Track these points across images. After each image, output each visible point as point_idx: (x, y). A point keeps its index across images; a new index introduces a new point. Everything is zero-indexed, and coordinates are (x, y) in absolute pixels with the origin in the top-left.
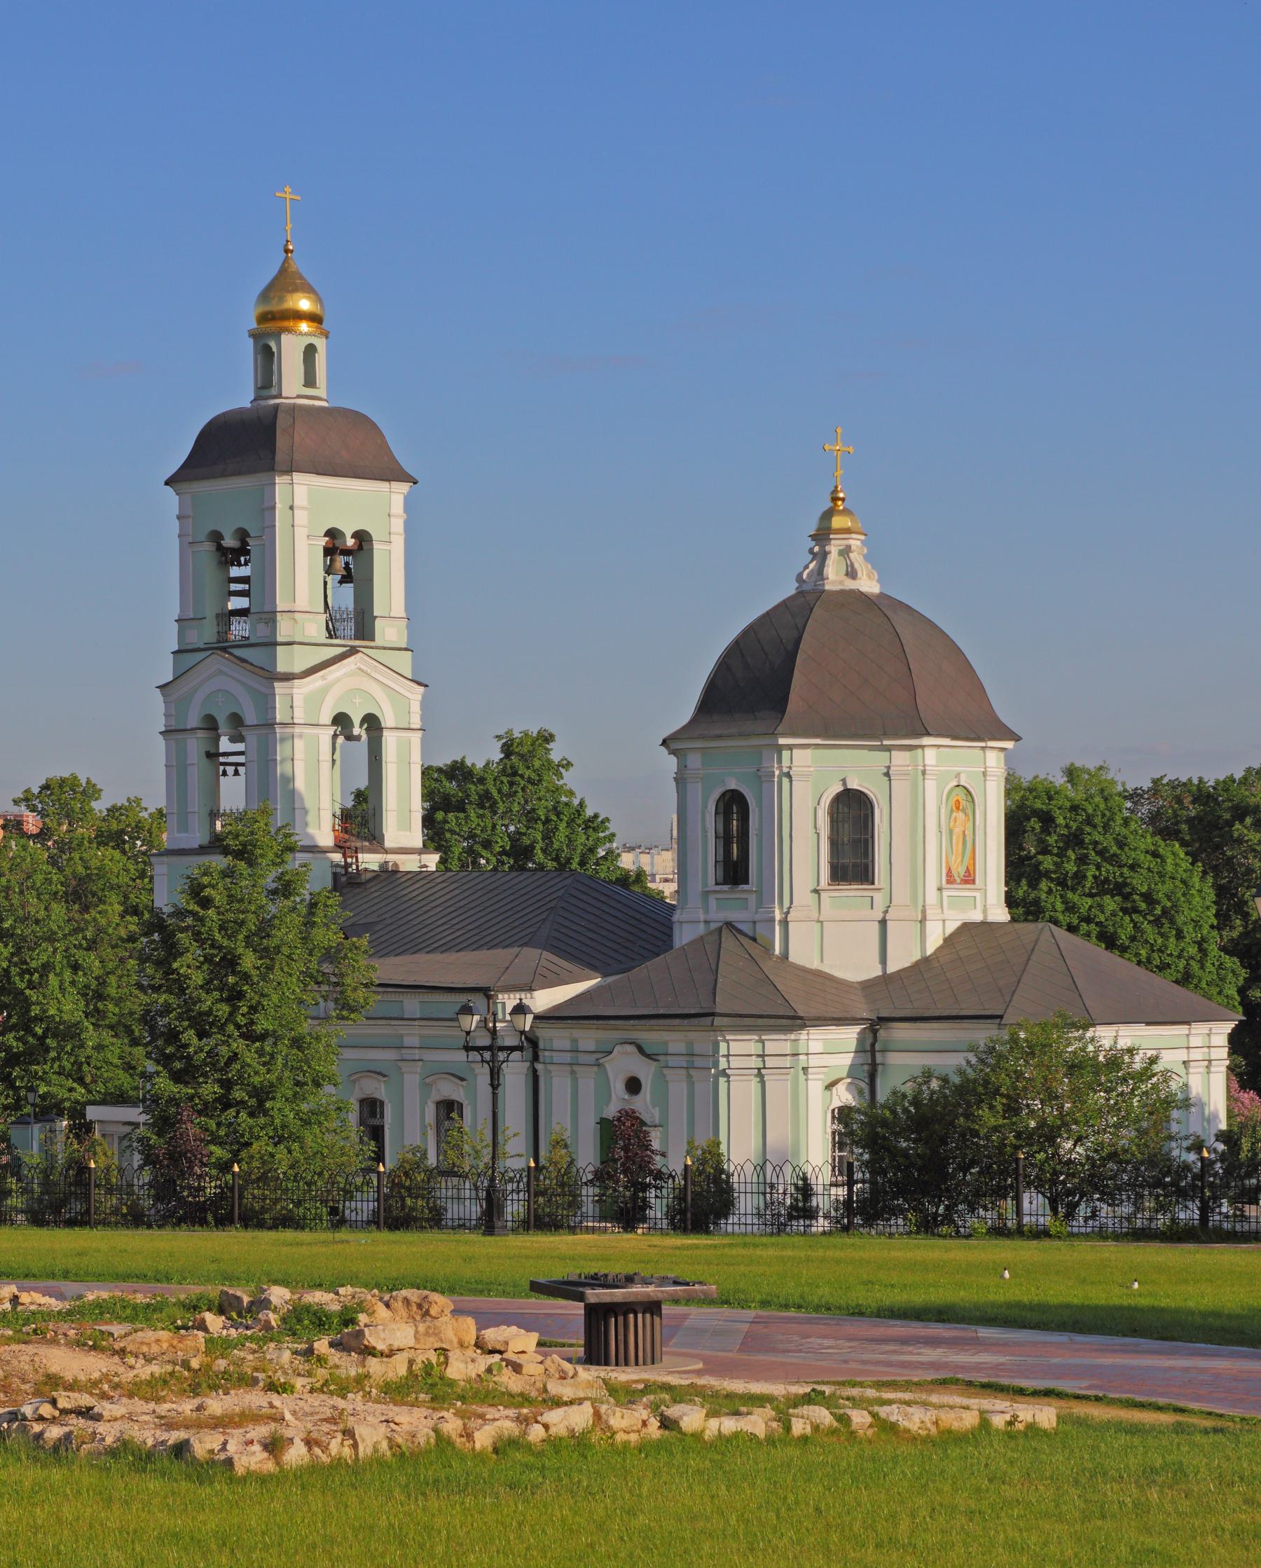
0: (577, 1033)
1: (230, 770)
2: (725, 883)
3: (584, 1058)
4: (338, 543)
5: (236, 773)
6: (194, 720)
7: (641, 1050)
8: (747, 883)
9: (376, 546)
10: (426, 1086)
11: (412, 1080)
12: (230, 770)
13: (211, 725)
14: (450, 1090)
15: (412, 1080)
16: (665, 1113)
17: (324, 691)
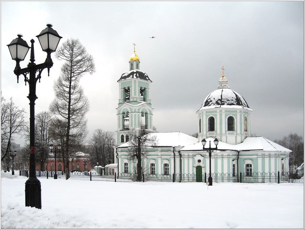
0: (189, 153)
1: (126, 120)
2: (210, 131)
3: (190, 157)
4: (142, 89)
5: (126, 121)
6: (121, 112)
7: (201, 156)
8: (214, 130)
9: (147, 90)
10: (162, 162)
11: (160, 160)
12: (126, 120)
13: (124, 113)
14: (166, 162)
15: (160, 160)
16: (205, 165)
17: (140, 108)
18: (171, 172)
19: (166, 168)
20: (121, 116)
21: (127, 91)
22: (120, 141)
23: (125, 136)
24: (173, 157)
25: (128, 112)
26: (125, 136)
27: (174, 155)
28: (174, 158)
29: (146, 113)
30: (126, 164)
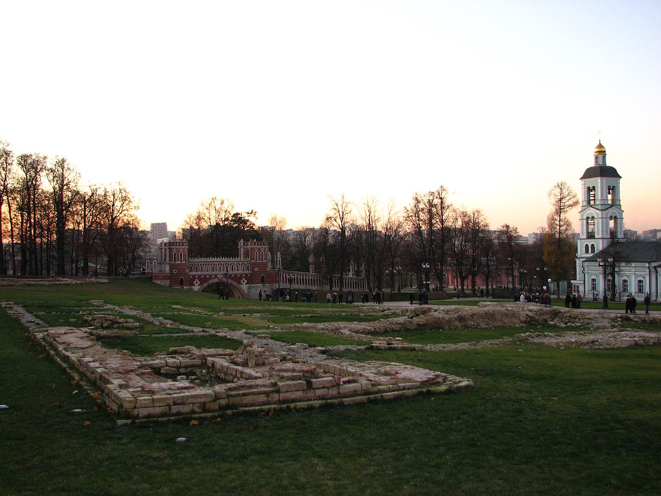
6: (585, 218)
13: (588, 218)
14: (640, 278)
15: (633, 277)
18: (647, 290)
19: (640, 285)
20: (585, 222)
21: (589, 190)
22: (584, 252)
23: (590, 246)
24: (648, 273)
25: (593, 218)
26: (590, 246)
27: (650, 272)
28: (650, 274)
29: (615, 218)
30: (594, 280)
